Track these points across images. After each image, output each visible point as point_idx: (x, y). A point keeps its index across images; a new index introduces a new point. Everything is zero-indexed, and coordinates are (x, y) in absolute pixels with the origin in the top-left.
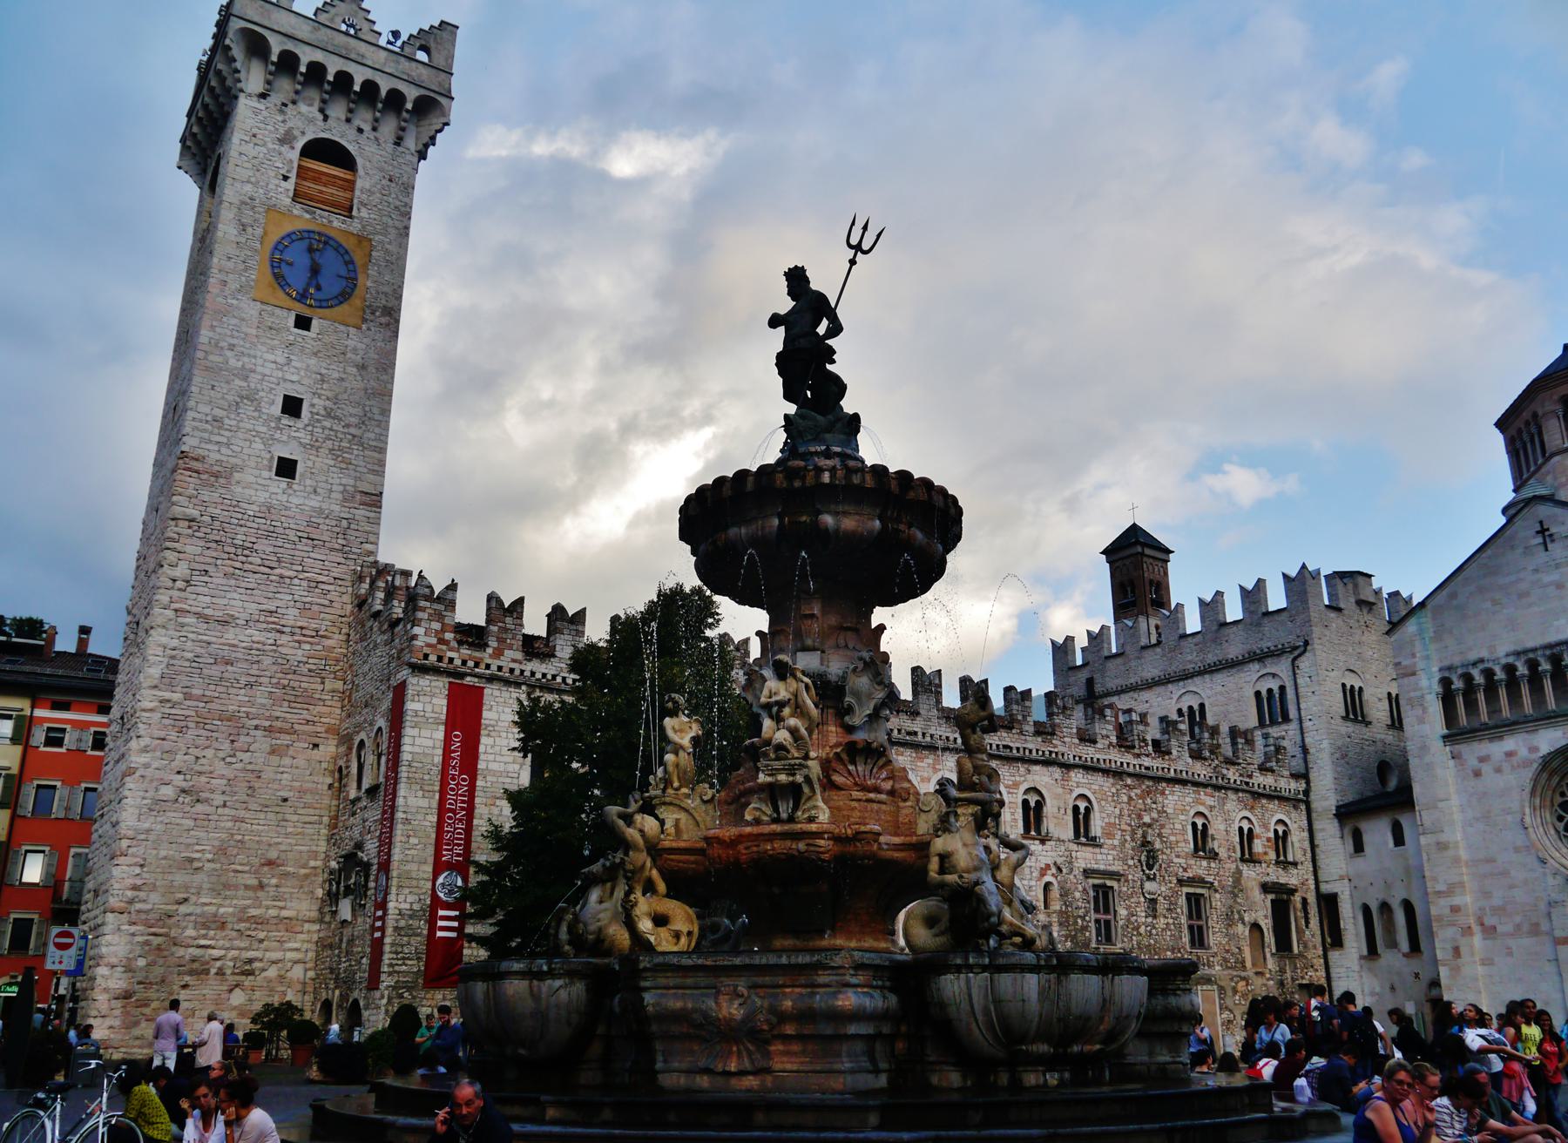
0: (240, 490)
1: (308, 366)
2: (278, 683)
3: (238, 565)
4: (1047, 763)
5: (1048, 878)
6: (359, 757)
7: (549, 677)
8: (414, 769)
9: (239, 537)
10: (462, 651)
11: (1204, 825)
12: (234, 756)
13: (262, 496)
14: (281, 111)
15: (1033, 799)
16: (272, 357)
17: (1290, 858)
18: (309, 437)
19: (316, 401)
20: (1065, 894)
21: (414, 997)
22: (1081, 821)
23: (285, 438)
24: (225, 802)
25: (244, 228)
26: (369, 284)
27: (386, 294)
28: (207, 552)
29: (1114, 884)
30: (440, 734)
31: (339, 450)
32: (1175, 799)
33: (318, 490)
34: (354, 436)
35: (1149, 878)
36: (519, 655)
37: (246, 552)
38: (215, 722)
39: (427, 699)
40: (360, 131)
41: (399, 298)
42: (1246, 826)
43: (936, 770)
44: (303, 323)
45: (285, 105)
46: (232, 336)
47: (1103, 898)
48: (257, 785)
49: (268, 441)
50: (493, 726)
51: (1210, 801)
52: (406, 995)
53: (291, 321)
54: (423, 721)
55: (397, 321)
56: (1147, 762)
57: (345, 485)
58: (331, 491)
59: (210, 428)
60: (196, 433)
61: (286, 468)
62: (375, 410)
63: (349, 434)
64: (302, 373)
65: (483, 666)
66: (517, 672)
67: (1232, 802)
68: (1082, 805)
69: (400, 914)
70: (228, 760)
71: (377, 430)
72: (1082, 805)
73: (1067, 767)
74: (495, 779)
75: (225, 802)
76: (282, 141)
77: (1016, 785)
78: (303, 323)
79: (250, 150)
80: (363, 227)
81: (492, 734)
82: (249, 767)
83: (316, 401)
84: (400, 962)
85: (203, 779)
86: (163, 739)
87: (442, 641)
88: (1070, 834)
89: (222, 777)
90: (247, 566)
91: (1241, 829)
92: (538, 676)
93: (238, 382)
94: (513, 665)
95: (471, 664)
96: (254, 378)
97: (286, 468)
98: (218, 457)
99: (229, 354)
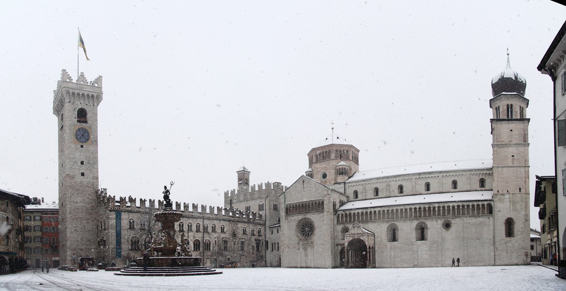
0: (76, 179)
3: (78, 192)
4: (217, 220)
5: (216, 239)
11: (245, 229)
13: (80, 180)
14: (73, 104)
15: (214, 226)
16: (77, 154)
17: (261, 234)
19: (86, 161)
20: (218, 241)
23: (82, 169)
25: (70, 130)
26: (92, 137)
27: (95, 138)
35: (234, 239)
40: (87, 104)
41: (97, 138)
42: (253, 229)
43: (196, 222)
44: (82, 146)
45: (73, 103)
46: (71, 152)
47: (225, 242)
49: (79, 170)
51: (247, 225)
53: (80, 147)
55: (97, 143)
58: (90, 177)
59: (70, 169)
60: (68, 170)
61: (83, 174)
67: (251, 225)
68: (223, 227)
72: (223, 227)
73: (220, 220)
76: (74, 110)
77: (211, 223)
78: (82, 146)
79: (69, 114)
80: (90, 125)
83: (86, 161)
90: (79, 193)
93: (73, 160)
97: (83, 174)
98: (72, 174)
99: (71, 155)
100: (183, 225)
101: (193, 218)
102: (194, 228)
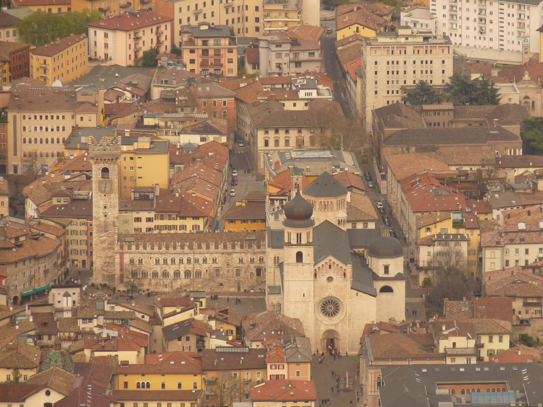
20: (210, 270)
22: (214, 261)
29: (220, 269)
30: (119, 259)
32: (234, 255)
42: (252, 258)
44: (105, 195)
51: (243, 255)
54: (117, 258)
56: (230, 250)
68: (215, 258)
78: (105, 195)
88: (212, 262)
91: (251, 259)
100: (175, 259)
101: (184, 254)
102: (185, 261)
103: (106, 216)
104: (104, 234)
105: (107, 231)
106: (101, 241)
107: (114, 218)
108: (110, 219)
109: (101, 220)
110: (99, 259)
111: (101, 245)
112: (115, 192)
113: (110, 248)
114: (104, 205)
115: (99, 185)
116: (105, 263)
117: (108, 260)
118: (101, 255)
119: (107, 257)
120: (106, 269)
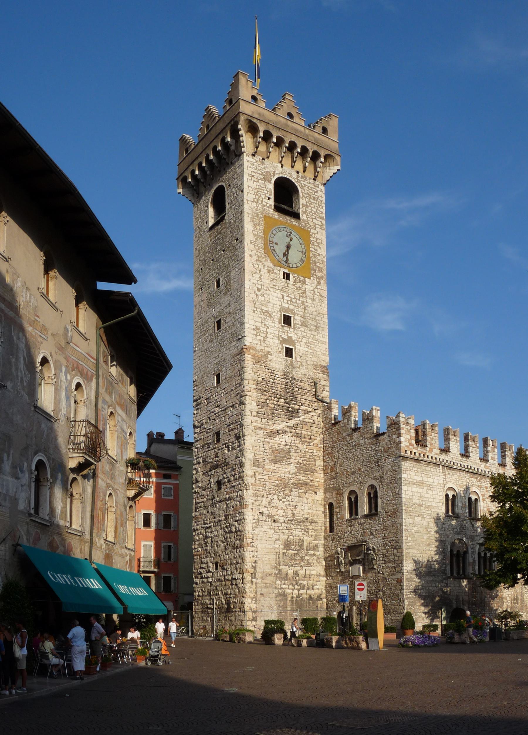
1: (291, 299)
2: (298, 462)
3: (276, 403)
6: (350, 499)
7: (449, 462)
8: (407, 506)
9: (274, 388)
10: (418, 449)
12: (285, 498)
18: (296, 336)
21: (415, 609)
24: (284, 520)
28: (263, 397)
31: (309, 343)
33: (303, 364)
34: (314, 336)
36: (438, 451)
37: (278, 396)
38: (276, 482)
39: (408, 472)
44: (287, 276)
48: (295, 512)
50: (432, 485)
52: (412, 607)
53: (282, 277)
57: (313, 361)
62: (321, 322)
63: (312, 334)
64: (289, 302)
65: (426, 457)
66: (438, 459)
69: (407, 572)
70: (283, 500)
71: (323, 333)
74: (434, 510)
75: (284, 520)
81: (432, 489)
82: (292, 503)
84: (409, 593)
85: (274, 509)
86: (258, 491)
87: (411, 445)
89: (281, 508)
92: (445, 461)
94: (437, 456)
95: (422, 455)
96: (270, 305)
98: (261, 348)
103: (289, 353)
104: (284, 425)
105: (293, 414)
106: (273, 450)
107: (315, 367)
108: (303, 370)
109: (272, 365)
110: (267, 526)
111: (274, 466)
112: (319, 274)
113: (306, 484)
114: (282, 309)
115: (265, 233)
116: (287, 545)
117: (298, 533)
118: (274, 512)
119: (293, 520)
120: (290, 572)
